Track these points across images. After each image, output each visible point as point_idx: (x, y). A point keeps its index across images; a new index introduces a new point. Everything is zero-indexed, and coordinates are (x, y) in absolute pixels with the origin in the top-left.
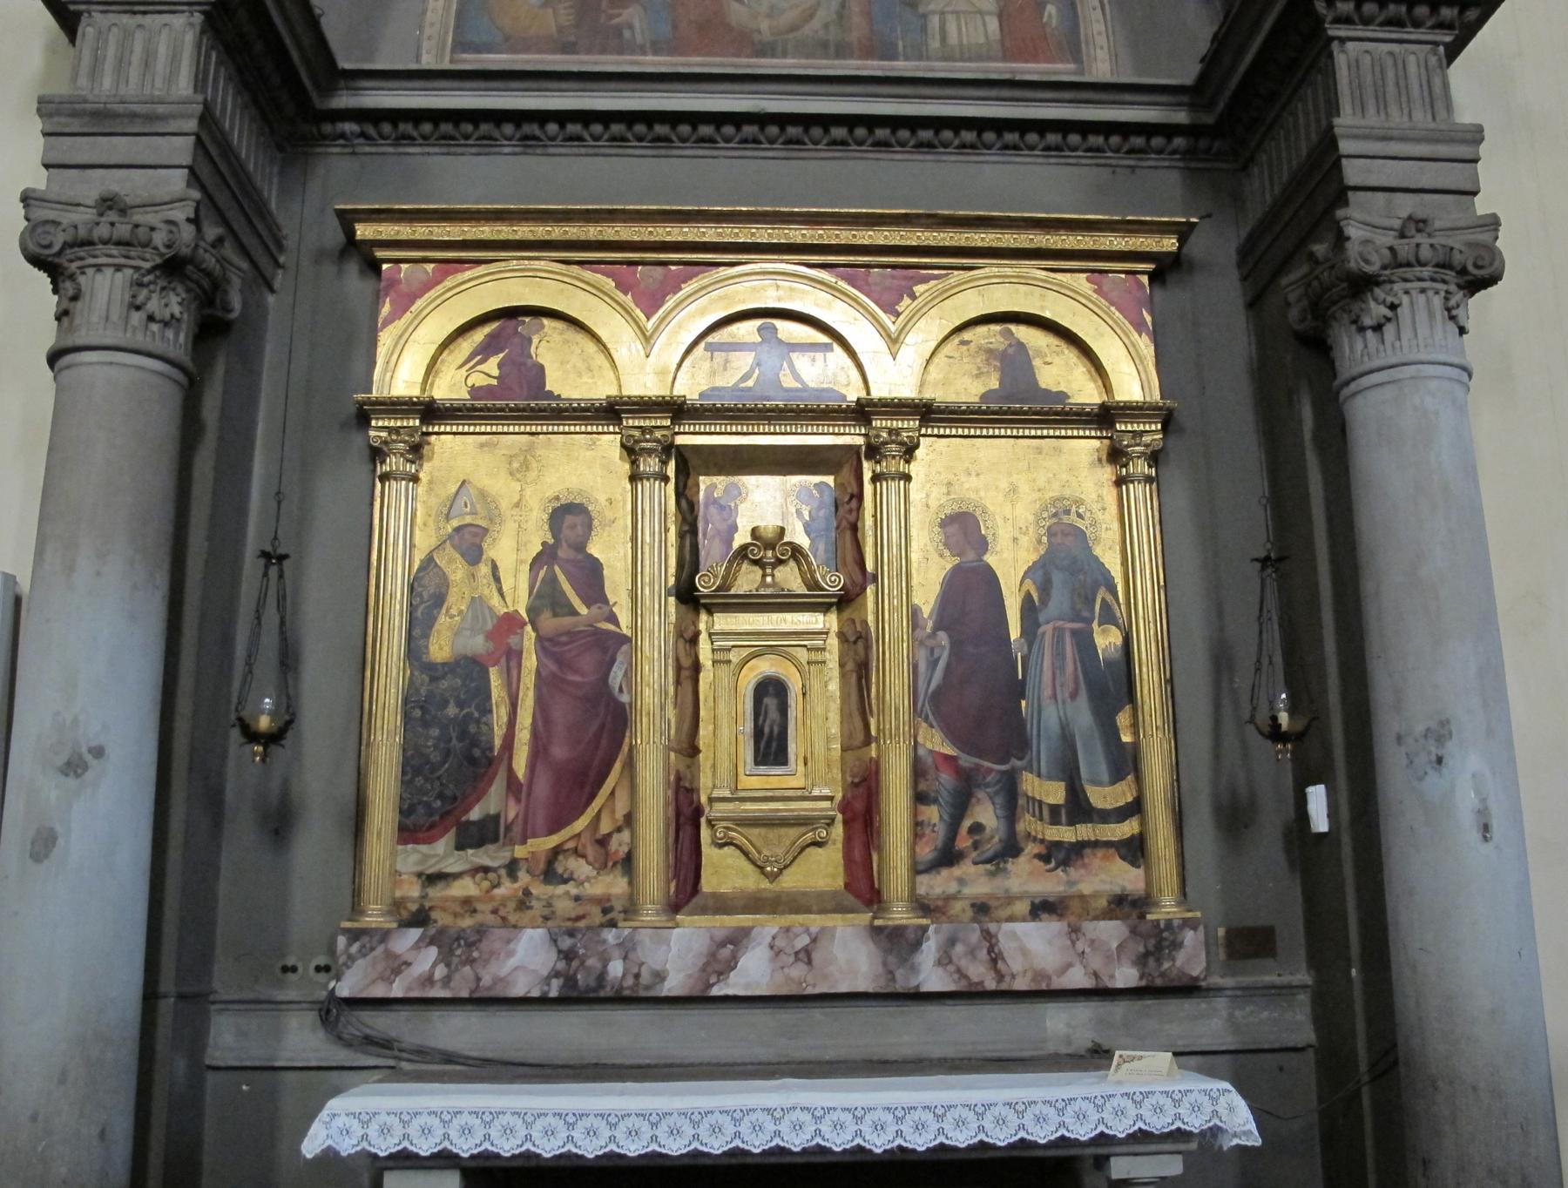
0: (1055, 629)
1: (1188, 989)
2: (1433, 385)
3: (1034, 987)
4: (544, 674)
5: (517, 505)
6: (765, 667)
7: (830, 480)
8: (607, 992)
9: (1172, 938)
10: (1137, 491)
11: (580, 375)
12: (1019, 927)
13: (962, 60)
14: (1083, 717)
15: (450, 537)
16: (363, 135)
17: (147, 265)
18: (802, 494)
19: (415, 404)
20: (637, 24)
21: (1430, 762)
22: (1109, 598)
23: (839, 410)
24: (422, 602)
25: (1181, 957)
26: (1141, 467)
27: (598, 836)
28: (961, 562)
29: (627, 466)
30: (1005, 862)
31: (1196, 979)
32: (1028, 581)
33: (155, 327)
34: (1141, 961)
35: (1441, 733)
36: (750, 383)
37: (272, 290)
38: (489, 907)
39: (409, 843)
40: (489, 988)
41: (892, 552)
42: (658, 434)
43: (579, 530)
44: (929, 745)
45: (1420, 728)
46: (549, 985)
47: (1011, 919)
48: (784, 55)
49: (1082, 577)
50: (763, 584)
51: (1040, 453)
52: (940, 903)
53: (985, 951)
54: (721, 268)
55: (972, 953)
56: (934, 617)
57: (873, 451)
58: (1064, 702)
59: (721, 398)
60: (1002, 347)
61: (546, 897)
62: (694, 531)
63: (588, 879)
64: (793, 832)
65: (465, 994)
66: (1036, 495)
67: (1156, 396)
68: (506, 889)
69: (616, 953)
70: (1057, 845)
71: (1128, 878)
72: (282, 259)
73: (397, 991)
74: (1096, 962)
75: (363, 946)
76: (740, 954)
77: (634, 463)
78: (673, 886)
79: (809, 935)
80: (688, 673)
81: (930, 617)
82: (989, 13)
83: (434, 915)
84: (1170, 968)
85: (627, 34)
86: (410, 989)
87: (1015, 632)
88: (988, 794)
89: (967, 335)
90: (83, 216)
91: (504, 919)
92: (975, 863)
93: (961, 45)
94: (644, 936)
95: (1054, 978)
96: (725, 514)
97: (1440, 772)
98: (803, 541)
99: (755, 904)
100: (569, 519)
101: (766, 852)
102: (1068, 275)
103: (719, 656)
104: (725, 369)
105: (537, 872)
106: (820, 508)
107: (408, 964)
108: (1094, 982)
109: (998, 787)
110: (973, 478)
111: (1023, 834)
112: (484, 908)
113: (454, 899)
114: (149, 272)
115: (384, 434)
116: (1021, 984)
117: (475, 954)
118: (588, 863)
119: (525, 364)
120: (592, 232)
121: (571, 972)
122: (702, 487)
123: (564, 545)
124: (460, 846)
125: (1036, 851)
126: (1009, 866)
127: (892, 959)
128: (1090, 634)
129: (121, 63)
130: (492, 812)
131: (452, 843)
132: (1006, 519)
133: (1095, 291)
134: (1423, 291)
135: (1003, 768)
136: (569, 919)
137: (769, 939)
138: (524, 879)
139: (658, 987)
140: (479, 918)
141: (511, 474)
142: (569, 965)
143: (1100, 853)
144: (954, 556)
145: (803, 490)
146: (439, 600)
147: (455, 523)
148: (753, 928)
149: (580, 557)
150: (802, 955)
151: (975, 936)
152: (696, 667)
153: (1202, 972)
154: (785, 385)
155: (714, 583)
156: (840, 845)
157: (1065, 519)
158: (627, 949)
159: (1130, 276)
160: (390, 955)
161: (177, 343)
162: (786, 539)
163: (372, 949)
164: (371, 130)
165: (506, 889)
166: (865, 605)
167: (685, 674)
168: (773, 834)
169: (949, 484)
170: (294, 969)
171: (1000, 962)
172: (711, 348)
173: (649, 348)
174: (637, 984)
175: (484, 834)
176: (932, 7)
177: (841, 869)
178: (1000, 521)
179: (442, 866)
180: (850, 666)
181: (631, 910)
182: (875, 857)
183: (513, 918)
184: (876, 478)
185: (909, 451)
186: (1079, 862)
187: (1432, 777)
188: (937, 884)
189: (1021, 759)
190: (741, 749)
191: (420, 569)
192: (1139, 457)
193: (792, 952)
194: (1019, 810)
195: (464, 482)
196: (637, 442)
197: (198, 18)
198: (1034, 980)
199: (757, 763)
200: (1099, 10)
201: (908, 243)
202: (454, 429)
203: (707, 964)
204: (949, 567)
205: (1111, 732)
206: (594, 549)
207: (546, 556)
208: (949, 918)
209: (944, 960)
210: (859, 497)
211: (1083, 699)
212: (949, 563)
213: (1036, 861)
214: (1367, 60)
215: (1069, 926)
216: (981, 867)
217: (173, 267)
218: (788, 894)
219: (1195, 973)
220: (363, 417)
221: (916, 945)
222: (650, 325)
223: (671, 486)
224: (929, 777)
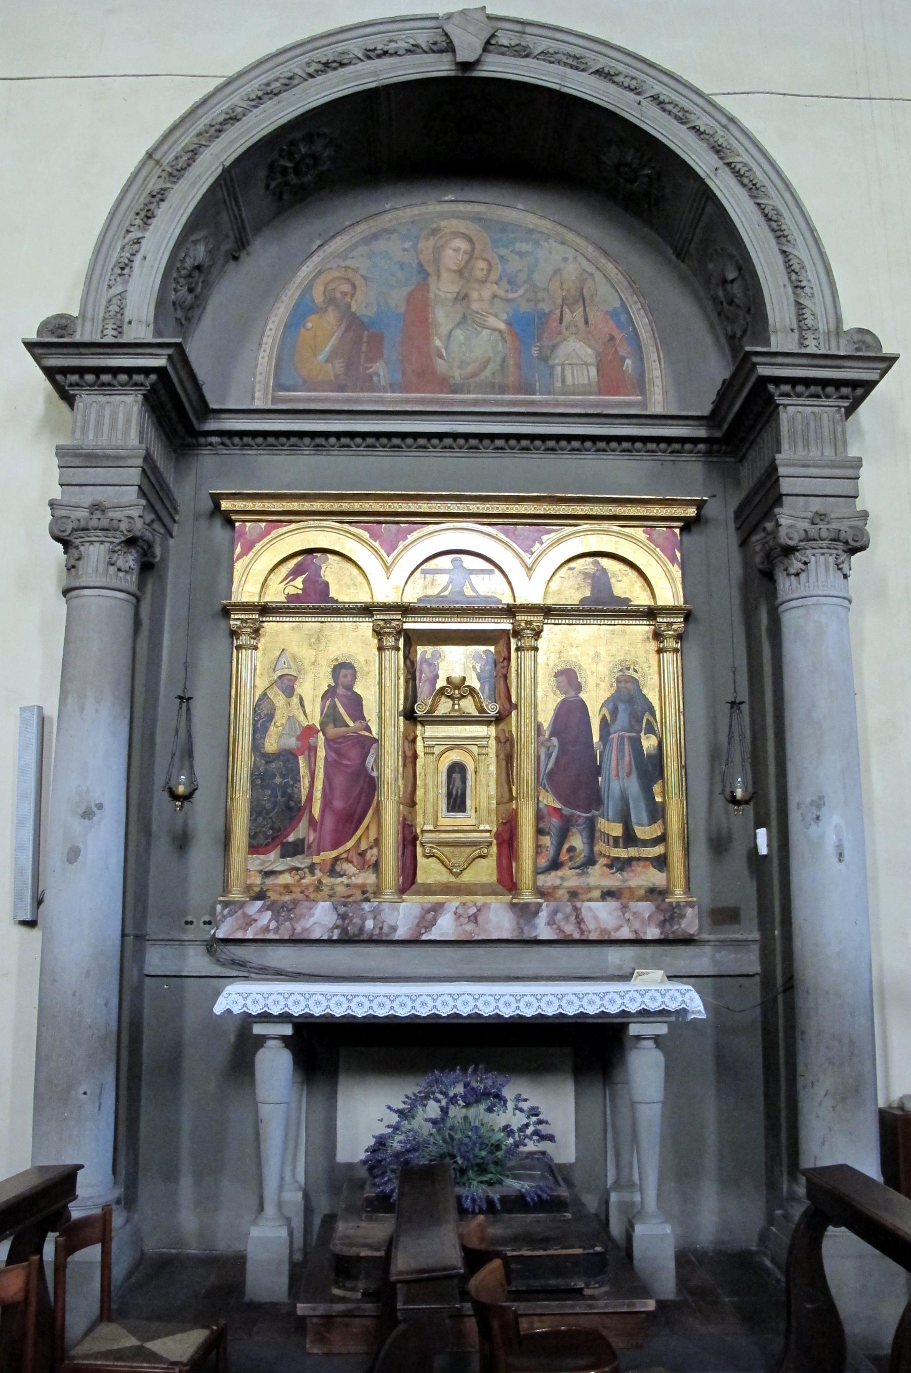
1: (688, 941)
2: (825, 608)
4: (329, 759)
5: (314, 663)
6: (454, 756)
7: (492, 648)
8: (365, 937)
10: (668, 657)
11: (349, 589)
13: (574, 394)
14: (633, 787)
15: (276, 681)
16: (223, 444)
17: (117, 541)
19: (256, 606)
20: (381, 373)
22: (651, 719)
23: (498, 609)
24: (261, 719)
25: (684, 923)
26: (671, 644)
29: (376, 641)
31: (693, 935)
33: (121, 574)
34: (662, 924)
35: (819, 803)
37: (171, 536)
38: (299, 890)
40: (301, 934)
41: (526, 693)
42: (394, 624)
43: (349, 678)
44: (545, 802)
45: (808, 800)
47: (590, 900)
48: (469, 392)
50: (453, 710)
52: (550, 891)
53: (574, 918)
54: (430, 526)
55: (567, 918)
57: (517, 633)
59: (430, 602)
60: (592, 571)
62: (414, 679)
63: (354, 875)
64: (468, 850)
65: (287, 937)
66: (611, 659)
69: (370, 916)
70: (618, 859)
71: (657, 878)
72: (177, 518)
73: (249, 935)
74: (636, 925)
77: (380, 640)
82: (592, 365)
83: (268, 894)
85: (375, 379)
86: (256, 934)
87: (596, 738)
89: (572, 564)
90: (83, 514)
91: (307, 896)
92: (571, 869)
93: (573, 385)
94: (386, 906)
95: (612, 933)
96: (432, 668)
98: (476, 685)
100: (343, 672)
101: (453, 861)
103: (428, 750)
104: (432, 584)
106: (485, 665)
107: (256, 921)
110: (574, 649)
113: (280, 885)
114: (119, 544)
115: (238, 623)
116: (593, 936)
118: (355, 866)
119: (317, 581)
120: (356, 506)
122: (419, 652)
124: (283, 856)
125: (605, 862)
126: (589, 870)
127: (522, 921)
128: (639, 740)
129: (99, 424)
130: (301, 837)
132: (592, 673)
133: (648, 539)
134: (823, 554)
137: (454, 909)
138: (318, 873)
140: (293, 896)
141: (310, 645)
143: (641, 864)
145: (477, 657)
146: (270, 717)
147: (279, 673)
148: (444, 903)
149: (350, 693)
150: (472, 918)
151: (569, 909)
152: (415, 756)
154: (467, 594)
156: (495, 858)
157: (627, 673)
160: (245, 915)
161: (130, 581)
162: (466, 684)
163: (236, 912)
164: (227, 441)
166: (511, 722)
167: (409, 760)
168: (457, 850)
169: (560, 652)
170: (192, 923)
172: (425, 572)
174: (380, 933)
175: (297, 849)
176: (557, 361)
177: (495, 871)
178: (589, 674)
180: (502, 756)
181: (378, 892)
182: (514, 865)
183: (312, 896)
184: (518, 649)
185: (537, 634)
186: (629, 869)
187: (814, 827)
188: (549, 880)
190: (439, 803)
191: (259, 700)
195: (283, 650)
196: (382, 628)
199: (448, 811)
200: (657, 362)
201: (538, 512)
202: (278, 619)
203: (419, 923)
204: (559, 700)
206: (358, 689)
207: (330, 693)
209: (551, 922)
210: (509, 659)
211: (634, 777)
212: (560, 698)
213: (605, 868)
214: (799, 416)
217: (131, 542)
218: (466, 884)
219: (691, 932)
220: (226, 612)
221: (536, 913)
223: (401, 653)
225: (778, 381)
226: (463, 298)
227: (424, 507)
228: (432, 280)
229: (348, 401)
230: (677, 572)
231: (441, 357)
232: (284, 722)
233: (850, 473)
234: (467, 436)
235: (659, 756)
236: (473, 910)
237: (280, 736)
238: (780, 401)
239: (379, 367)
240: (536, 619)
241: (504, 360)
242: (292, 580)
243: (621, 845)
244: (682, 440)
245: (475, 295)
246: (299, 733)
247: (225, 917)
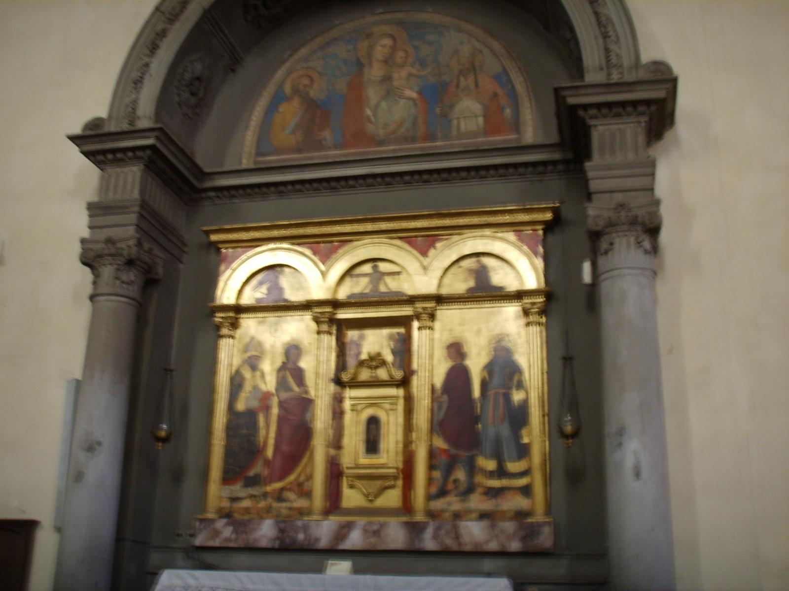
12: (470, 524)
14: (505, 430)
16: (218, 197)
18: (391, 337)
34: (524, 539)
35: (621, 432)
37: (182, 263)
47: (471, 520)
64: (379, 483)
68: (262, 504)
71: (520, 502)
72: (186, 249)
73: (217, 543)
80: (338, 414)
87: (476, 392)
115: (221, 320)
116: (468, 548)
129: (116, 186)
147: (249, 354)
158: (305, 528)
161: (134, 291)
165: (262, 504)
184: (420, 328)
185: (432, 317)
188: (438, 505)
197: (142, 166)
205: (517, 436)
207: (283, 368)
209: (435, 537)
216: (458, 498)
217: (130, 263)
225: (586, 107)
226: (387, 79)
227: (348, 228)
228: (366, 70)
229: (305, 159)
230: (540, 263)
231: (370, 121)
233: (648, 170)
234: (383, 175)
235: (525, 405)
236: (375, 527)
237: (247, 399)
238: (592, 122)
239: (327, 135)
240: (430, 305)
241: (416, 119)
244: (544, 163)
245: (396, 76)
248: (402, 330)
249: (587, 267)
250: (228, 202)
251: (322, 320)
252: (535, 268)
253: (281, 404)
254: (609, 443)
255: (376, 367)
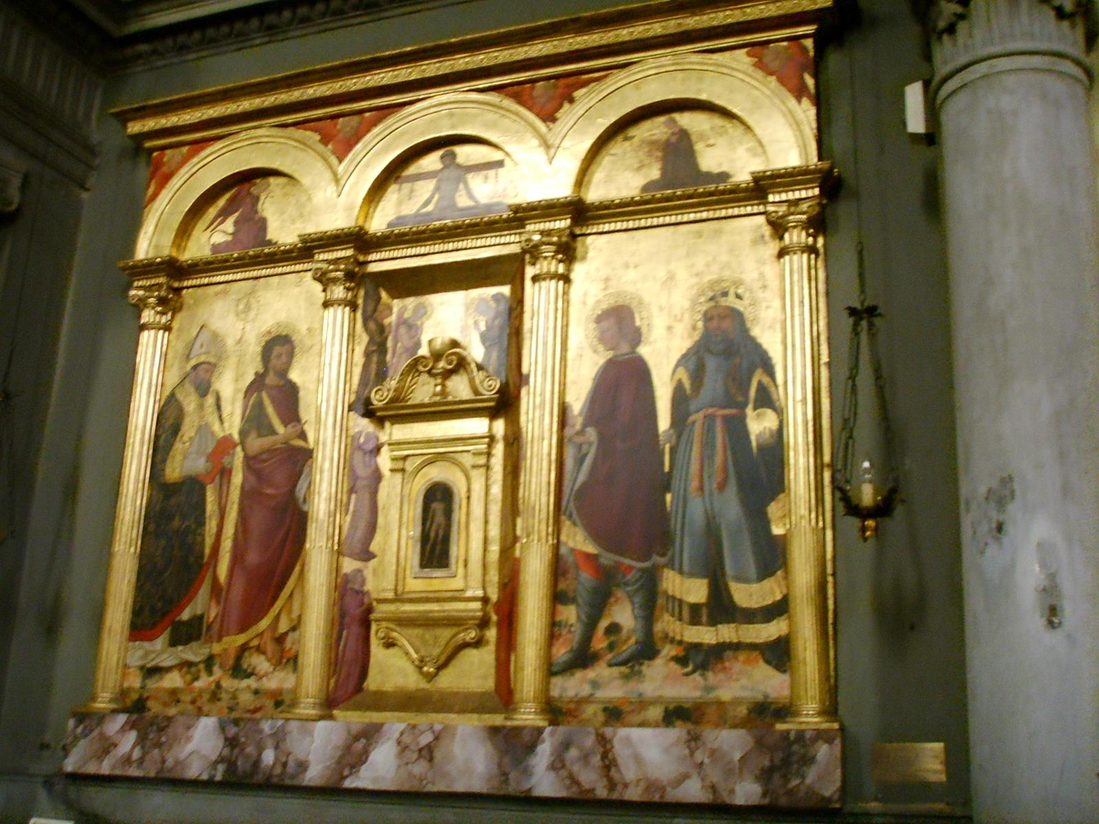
0: (705, 417)
2: (1010, 80)
3: (645, 799)
6: (435, 473)
8: (259, 778)
9: (802, 751)
12: (635, 733)
14: (731, 508)
21: (990, 531)
22: (766, 380)
25: (811, 775)
27: (277, 635)
28: (615, 356)
30: (641, 664)
31: (829, 800)
32: (681, 370)
34: (765, 776)
35: (1002, 494)
36: (430, 208)
37: (82, 187)
39: (136, 641)
40: (170, 770)
43: (284, 359)
44: (571, 544)
45: (983, 490)
46: (215, 769)
47: (642, 724)
49: (737, 360)
51: (700, 237)
52: (572, 706)
53: (599, 757)
55: (585, 758)
56: (584, 414)
58: (711, 494)
60: (664, 137)
61: (232, 690)
63: (266, 674)
64: (446, 634)
65: (152, 774)
67: (813, 159)
68: (204, 682)
69: (270, 743)
70: (697, 647)
73: (105, 768)
74: (715, 776)
75: (85, 728)
76: (371, 748)
78: (332, 681)
79: (433, 732)
81: (580, 414)
83: (150, 704)
84: (798, 786)
86: (114, 767)
87: (664, 422)
88: (627, 593)
92: (610, 665)
94: (293, 726)
95: (669, 789)
96: (413, 332)
97: (998, 539)
99: (408, 702)
102: (727, 54)
105: (228, 668)
106: (495, 318)
107: (115, 745)
108: (711, 797)
109: (639, 584)
111: (660, 635)
112: (187, 698)
113: (165, 690)
117: (164, 739)
118: (268, 660)
121: (234, 758)
122: (395, 310)
123: (271, 373)
124: (173, 643)
125: (673, 653)
126: (644, 668)
128: (742, 419)
130: (199, 612)
131: (167, 642)
135: (646, 564)
136: (249, 711)
137: (397, 735)
138: (217, 672)
139: (301, 776)
140: (181, 706)
141: (237, 315)
142: (232, 751)
143: (742, 656)
144: (608, 350)
146: (176, 430)
147: (193, 362)
148: (382, 725)
150: (425, 752)
151: (590, 741)
152: (377, 477)
153: (835, 792)
155: (387, 396)
157: (724, 302)
158: (279, 738)
159: (792, 43)
160: (103, 737)
163: (91, 731)
165: (204, 682)
168: (429, 635)
169: (607, 279)
171: (613, 769)
173: (340, 189)
174: (283, 773)
175: (186, 634)
177: (493, 671)
178: (655, 311)
179: (158, 660)
180: (509, 468)
182: (513, 658)
186: (719, 666)
187: (991, 551)
188: (570, 687)
189: (663, 555)
192: (795, 227)
193: (416, 749)
194: (657, 612)
198: (647, 789)
203: (342, 757)
206: (294, 375)
207: (258, 384)
208: (580, 722)
209: (557, 764)
211: (732, 491)
215: (689, 733)
216: (615, 671)
219: (827, 793)
221: (531, 748)
222: (341, 169)
224: (569, 576)
230: (807, 112)
232: (193, 434)
235: (776, 448)
236: (426, 739)
242: (220, 224)
243: (704, 619)
246: (210, 450)
247: (77, 739)
248: (506, 290)
249: (914, 95)
250: (176, 60)
251: (333, 275)
252: (797, 125)
253: (251, 462)
254: (972, 523)
255: (447, 374)
